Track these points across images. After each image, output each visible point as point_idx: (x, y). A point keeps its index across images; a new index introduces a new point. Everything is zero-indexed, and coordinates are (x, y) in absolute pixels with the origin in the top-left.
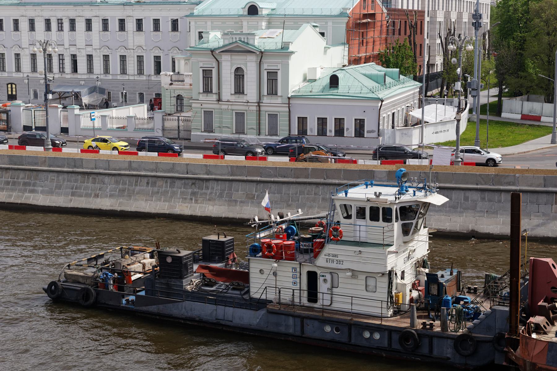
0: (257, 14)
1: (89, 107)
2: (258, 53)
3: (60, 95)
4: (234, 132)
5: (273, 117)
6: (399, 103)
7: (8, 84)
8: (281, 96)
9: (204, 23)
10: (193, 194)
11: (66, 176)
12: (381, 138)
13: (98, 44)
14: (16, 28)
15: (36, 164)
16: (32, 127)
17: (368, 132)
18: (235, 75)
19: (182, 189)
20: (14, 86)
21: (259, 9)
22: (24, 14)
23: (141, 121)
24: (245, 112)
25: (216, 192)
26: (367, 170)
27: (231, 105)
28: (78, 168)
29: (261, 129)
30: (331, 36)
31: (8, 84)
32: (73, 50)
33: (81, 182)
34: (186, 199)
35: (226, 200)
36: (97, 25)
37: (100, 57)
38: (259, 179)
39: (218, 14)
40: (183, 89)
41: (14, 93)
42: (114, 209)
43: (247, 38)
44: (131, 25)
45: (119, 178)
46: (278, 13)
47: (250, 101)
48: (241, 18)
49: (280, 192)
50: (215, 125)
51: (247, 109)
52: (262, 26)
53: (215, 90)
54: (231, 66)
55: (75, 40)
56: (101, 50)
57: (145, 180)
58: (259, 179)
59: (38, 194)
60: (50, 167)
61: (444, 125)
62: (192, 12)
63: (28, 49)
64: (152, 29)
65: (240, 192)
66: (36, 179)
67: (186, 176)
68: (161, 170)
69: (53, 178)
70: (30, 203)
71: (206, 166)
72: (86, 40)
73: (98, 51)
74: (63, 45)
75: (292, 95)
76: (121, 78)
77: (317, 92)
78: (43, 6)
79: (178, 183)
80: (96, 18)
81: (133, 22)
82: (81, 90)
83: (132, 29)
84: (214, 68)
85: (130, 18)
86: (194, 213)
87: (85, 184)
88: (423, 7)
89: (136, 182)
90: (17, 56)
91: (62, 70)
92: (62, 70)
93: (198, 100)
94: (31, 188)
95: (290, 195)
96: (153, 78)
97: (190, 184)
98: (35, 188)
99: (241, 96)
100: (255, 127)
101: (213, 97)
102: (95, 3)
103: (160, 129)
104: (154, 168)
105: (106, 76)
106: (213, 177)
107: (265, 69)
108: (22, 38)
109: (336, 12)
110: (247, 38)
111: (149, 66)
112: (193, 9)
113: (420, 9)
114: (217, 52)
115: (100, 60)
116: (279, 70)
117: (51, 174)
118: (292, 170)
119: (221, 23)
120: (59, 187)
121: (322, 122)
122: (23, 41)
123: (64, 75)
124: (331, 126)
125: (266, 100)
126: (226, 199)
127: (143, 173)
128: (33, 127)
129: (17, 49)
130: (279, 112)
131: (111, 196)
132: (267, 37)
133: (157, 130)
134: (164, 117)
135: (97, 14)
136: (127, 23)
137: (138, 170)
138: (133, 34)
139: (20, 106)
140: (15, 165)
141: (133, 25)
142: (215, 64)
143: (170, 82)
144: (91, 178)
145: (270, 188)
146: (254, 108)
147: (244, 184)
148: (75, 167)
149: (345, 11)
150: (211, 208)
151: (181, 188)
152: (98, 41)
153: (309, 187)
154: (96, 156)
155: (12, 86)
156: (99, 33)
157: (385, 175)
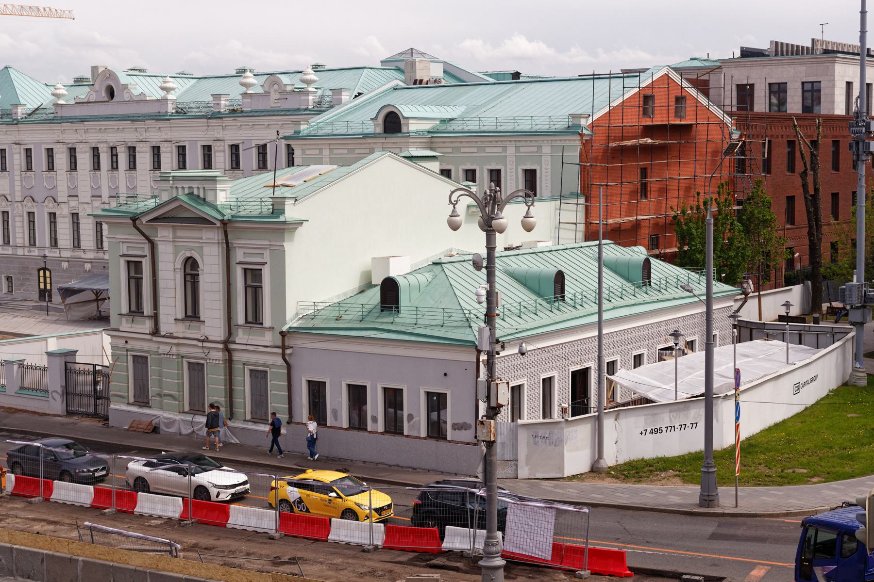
0: (399, 130)
2: (218, 224)
3: (96, 294)
4: (187, 409)
7: (39, 270)
8: (271, 329)
18: (185, 275)
20: (48, 273)
21: (402, 121)
27: (178, 345)
29: (235, 405)
31: (39, 270)
41: (48, 287)
43: (204, 188)
47: (210, 338)
48: (369, 141)
50: (153, 390)
53: (147, 308)
54: (176, 254)
61: (679, 410)
63: (67, 205)
75: (295, 325)
78: (86, 123)
80: (166, 144)
81: (224, 152)
84: (145, 256)
85: (218, 143)
90: (53, 216)
99: (194, 324)
102: (164, 116)
107: (240, 263)
109: (561, 124)
110: (204, 188)
112: (298, 123)
114: (144, 220)
116: (264, 264)
118: (42, 561)
121: (357, 395)
122: (59, 188)
124: (375, 406)
125: (241, 337)
129: (51, 205)
136: (215, 152)
142: (147, 251)
149: (576, 122)
155: (45, 274)
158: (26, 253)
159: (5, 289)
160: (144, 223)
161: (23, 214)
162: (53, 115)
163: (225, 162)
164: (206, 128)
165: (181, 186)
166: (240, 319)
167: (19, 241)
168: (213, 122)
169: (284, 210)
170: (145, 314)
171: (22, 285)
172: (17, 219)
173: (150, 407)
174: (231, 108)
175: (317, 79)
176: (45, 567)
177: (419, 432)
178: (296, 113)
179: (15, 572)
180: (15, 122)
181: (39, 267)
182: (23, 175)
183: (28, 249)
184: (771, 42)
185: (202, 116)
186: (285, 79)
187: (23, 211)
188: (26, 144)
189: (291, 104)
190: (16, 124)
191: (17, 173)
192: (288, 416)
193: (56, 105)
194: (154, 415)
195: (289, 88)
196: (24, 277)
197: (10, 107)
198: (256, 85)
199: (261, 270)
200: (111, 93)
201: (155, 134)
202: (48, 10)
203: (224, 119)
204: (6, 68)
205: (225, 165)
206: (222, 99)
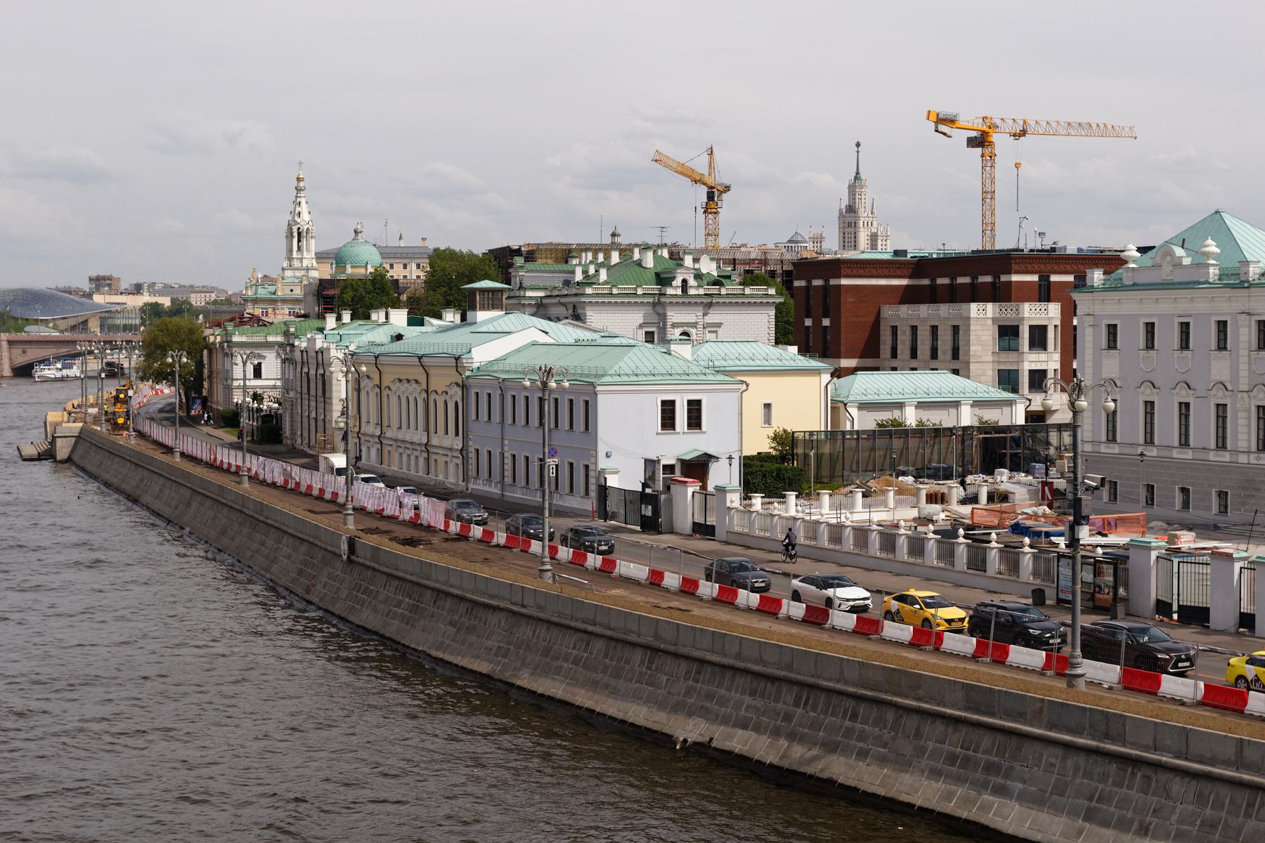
11: (1081, 759)
15: (1020, 716)
16: (1171, 605)
28: (1113, 740)
33: (1114, 784)
45: (1207, 787)
59: (1011, 799)
60: (1050, 730)
66: (1014, 758)
69: (1053, 761)
70: (986, 823)
87: (1124, 790)
94: (1000, 780)
98: (1009, 782)
120: (1060, 789)
128: (1175, 608)
139: (1150, 549)
144: (1139, 774)
148: (1107, 736)
158: (1253, 461)
159: (1215, 509)
161: (1250, 408)
167: (1242, 445)
171: (1243, 504)
172: (1240, 415)
180: (1246, 285)
182: (1253, 357)
183: (1256, 455)
187: (1249, 404)
196: (1247, 493)
197: (1237, 265)
202: (1102, 126)
204: (1217, 212)
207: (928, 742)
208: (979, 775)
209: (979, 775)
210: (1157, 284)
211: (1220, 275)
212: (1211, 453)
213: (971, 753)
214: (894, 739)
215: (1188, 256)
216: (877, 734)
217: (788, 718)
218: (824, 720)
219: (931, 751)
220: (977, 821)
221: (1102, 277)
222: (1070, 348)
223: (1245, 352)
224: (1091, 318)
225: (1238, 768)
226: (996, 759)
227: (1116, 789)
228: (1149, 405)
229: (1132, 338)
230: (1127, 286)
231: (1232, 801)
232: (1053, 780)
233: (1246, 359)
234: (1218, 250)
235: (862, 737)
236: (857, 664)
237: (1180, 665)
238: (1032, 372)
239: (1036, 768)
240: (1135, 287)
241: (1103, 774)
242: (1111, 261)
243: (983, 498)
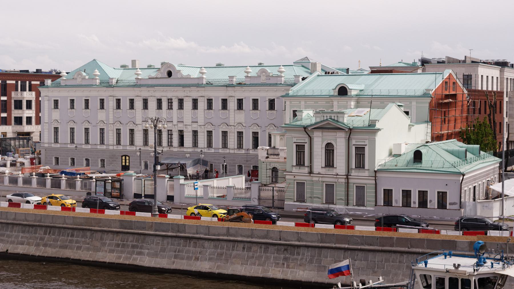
0: (347, 94)
1: (193, 178)
2: (347, 130)
3: (167, 166)
4: (324, 202)
5: (361, 189)
6: (480, 178)
7: (122, 156)
9: (298, 103)
10: (285, 259)
11: (170, 240)
12: (462, 210)
13: (203, 121)
14: (132, 107)
15: (144, 228)
16: (141, 195)
17: (450, 204)
18: (326, 150)
19: (275, 255)
20: (127, 158)
22: (139, 94)
23: (239, 191)
24: (335, 184)
25: (306, 258)
26: (450, 241)
27: (322, 177)
28: (181, 233)
29: (349, 200)
30: (415, 115)
31: (122, 156)
32: (181, 127)
33: (183, 246)
34: (278, 264)
35: (315, 266)
36: (202, 105)
37: (204, 133)
38: (346, 246)
39: (311, 94)
40: (278, 162)
41: (127, 164)
42: (212, 272)
43: (337, 116)
44: (232, 105)
45: (217, 243)
46: (366, 94)
47: (339, 174)
48: (332, 98)
49: (366, 260)
50: (307, 195)
51: (337, 181)
52: (351, 105)
53: (307, 163)
55: (183, 117)
56: (205, 127)
57: (241, 245)
58: (346, 246)
59: (144, 255)
60: (156, 232)
62: (287, 93)
64: (251, 107)
65: (329, 259)
66: (143, 242)
67: (279, 242)
68: (256, 236)
69: (159, 241)
70: (137, 264)
71: (298, 233)
72: (192, 117)
73: (203, 127)
74: (172, 122)
75: (379, 168)
76: (223, 152)
77: (402, 166)
78: (155, 87)
79: (271, 248)
80: (201, 98)
81: (234, 102)
82: (186, 162)
83: (233, 108)
84: (306, 143)
85: (231, 98)
86: (285, 278)
87: (187, 248)
88: (502, 88)
89: (233, 247)
90: (132, 131)
91: (170, 144)
92: (170, 144)
93: (292, 172)
94: (139, 250)
95: (376, 262)
96: (251, 152)
97: (283, 250)
98: (142, 250)
99: (331, 169)
100: (343, 198)
101: (305, 170)
102: (201, 85)
103: (256, 198)
104: (250, 234)
105: (209, 150)
106: (304, 243)
107: (354, 145)
108: (137, 115)
109: (420, 93)
111: (248, 141)
112: (289, 90)
113: (499, 90)
115: (204, 135)
116: (366, 145)
117: (157, 238)
118: (378, 239)
119: (313, 103)
120: (163, 250)
121: (407, 194)
122: (137, 118)
123: (172, 149)
124: (415, 198)
125: (354, 173)
126: (316, 265)
127: (239, 239)
128: (143, 195)
130: (366, 184)
131: (210, 259)
132: (355, 115)
133: (254, 199)
134: (260, 188)
135: (203, 94)
136: (229, 102)
137: (235, 236)
138: (234, 112)
139: (132, 176)
140: (126, 228)
141: (234, 104)
142: (307, 140)
143: (267, 156)
144: (192, 242)
145: (357, 255)
146: (343, 181)
147: (333, 251)
148: (178, 231)
149: (428, 92)
150: (301, 273)
151: (274, 254)
152: (203, 119)
153: (393, 256)
154: (197, 222)
155: (126, 158)
156: (204, 111)
157: (466, 245)
159: (100, 166)
160: (309, 129)
161: (114, 130)
162: (136, 83)
163: (234, 106)
164: (226, 91)
165: (326, 115)
166: (353, 165)
168: (229, 88)
169: (376, 125)
170: (306, 165)
171: (111, 163)
172: (110, 132)
173: (306, 202)
174: (239, 82)
175: (285, 70)
176: (379, 241)
177: (435, 206)
178: (275, 85)
179: (364, 244)
180: (112, 86)
181: (122, 155)
183: (117, 146)
184: (446, 57)
185: (223, 85)
186: (269, 70)
187: (114, 128)
188: (117, 97)
189: (272, 81)
190: (113, 87)
191: (111, 110)
192: (375, 203)
193: (137, 79)
194: (308, 206)
195: (271, 75)
198: (253, 72)
199: (364, 147)
200: (170, 74)
201: (195, 93)
203: (236, 87)
204: (94, 60)
205: (235, 108)
206: (234, 78)
207: (106, 241)
208: (130, 249)
209: (130, 249)
210: (75, 85)
211: (100, 82)
212: (83, 145)
213: (125, 243)
214: (92, 241)
215: (87, 75)
216: (83, 240)
217: (42, 239)
218: (59, 238)
219: (108, 244)
220: (133, 264)
221: (51, 82)
222: (38, 110)
223: (112, 110)
224: (48, 97)
225: (227, 236)
226: (136, 243)
227: (184, 248)
228: (72, 129)
229: (65, 105)
230: (63, 86)
231: (227, 246)
232: (160, 248)
233: (112, 113)
234: (99, 74)
235: (77, 242)
236: (72, 218)
237: (169, 211)
238: (27, 117)
239: (152, 245)
240: (66, 86)
241: (179, 244)
242: (56, 76)
243: (8, 164)
